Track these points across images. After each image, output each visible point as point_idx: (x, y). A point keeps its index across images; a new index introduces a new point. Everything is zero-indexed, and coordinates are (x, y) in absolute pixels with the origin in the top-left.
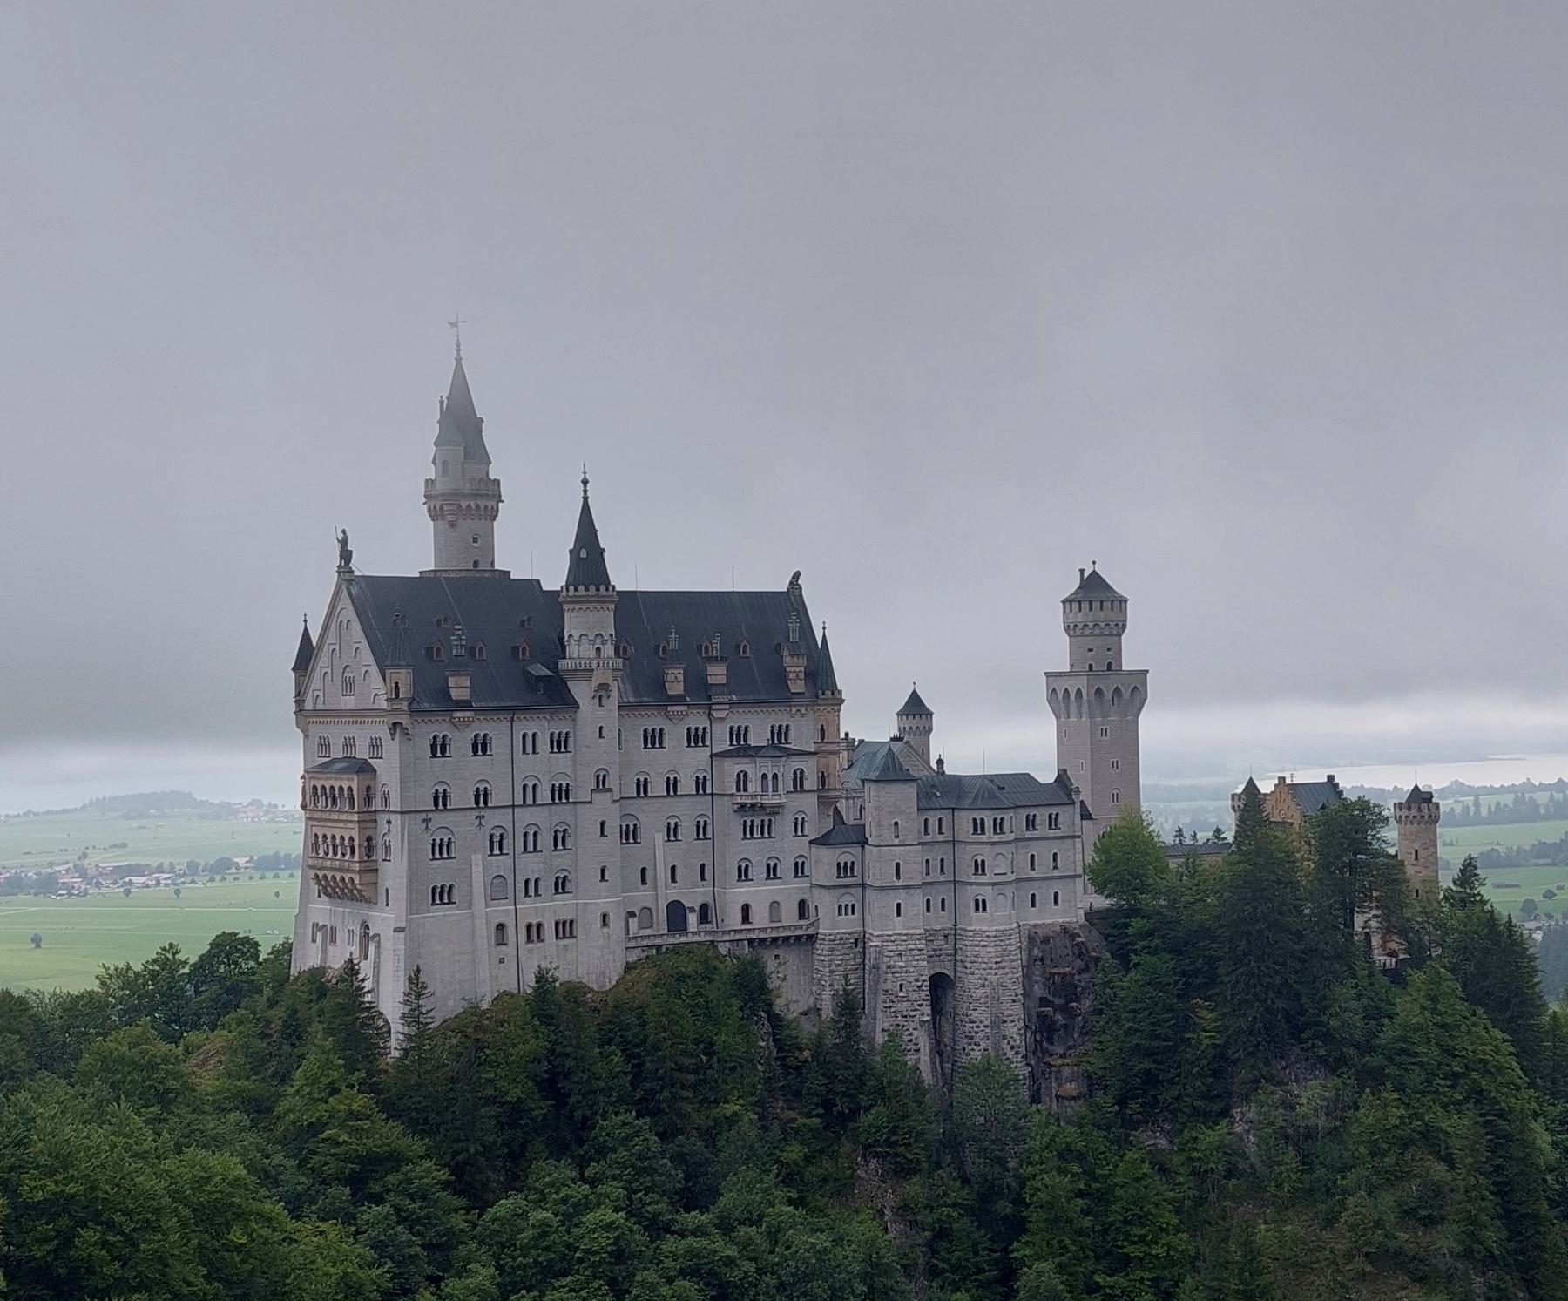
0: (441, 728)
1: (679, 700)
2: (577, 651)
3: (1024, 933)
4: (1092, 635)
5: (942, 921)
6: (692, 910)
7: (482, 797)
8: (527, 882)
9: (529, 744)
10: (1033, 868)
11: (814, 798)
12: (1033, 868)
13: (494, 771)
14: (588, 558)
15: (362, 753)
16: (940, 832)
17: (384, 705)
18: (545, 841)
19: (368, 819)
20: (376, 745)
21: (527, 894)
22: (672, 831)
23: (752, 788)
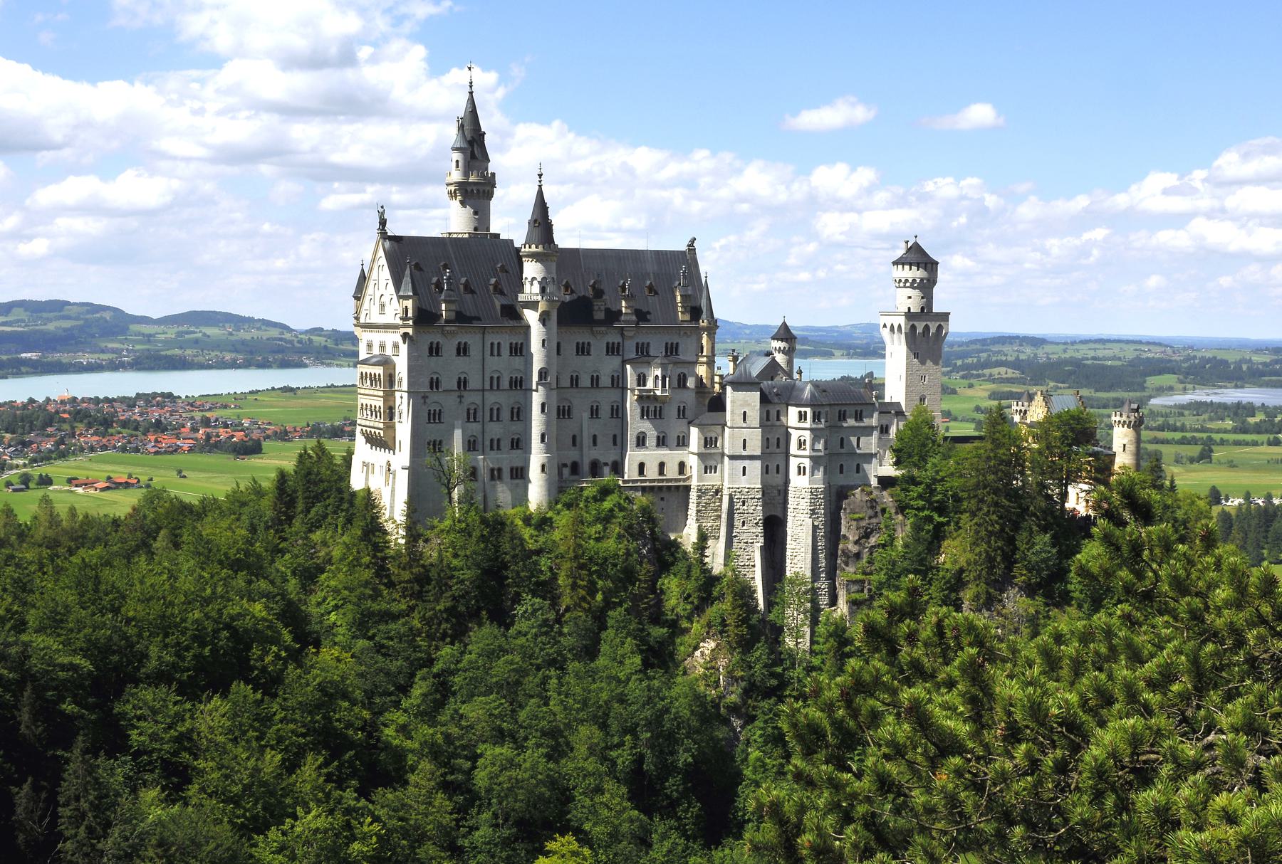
0: (437, 338)
1: (600, 323)
2: (531, 291)
3: (833, 490)
4: (912, 287)
5: (777, 480)
6: (606, 464)
7: (462, 384)
8: (492, 440)
9: (496, 350)
10: (842, 446)
11: (693, 395)
12: (842, 446)
13: (468, 367)
14: (541, 223)
15: (389, 351)
16: (778, 419)
17: (401, 322)
18: (505, 414)
19: (389, 396)
20: (396, 347)
21: (492, 449)
22: (595, 413)
23: (650, 384)
